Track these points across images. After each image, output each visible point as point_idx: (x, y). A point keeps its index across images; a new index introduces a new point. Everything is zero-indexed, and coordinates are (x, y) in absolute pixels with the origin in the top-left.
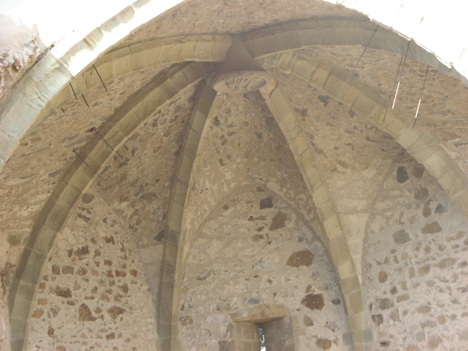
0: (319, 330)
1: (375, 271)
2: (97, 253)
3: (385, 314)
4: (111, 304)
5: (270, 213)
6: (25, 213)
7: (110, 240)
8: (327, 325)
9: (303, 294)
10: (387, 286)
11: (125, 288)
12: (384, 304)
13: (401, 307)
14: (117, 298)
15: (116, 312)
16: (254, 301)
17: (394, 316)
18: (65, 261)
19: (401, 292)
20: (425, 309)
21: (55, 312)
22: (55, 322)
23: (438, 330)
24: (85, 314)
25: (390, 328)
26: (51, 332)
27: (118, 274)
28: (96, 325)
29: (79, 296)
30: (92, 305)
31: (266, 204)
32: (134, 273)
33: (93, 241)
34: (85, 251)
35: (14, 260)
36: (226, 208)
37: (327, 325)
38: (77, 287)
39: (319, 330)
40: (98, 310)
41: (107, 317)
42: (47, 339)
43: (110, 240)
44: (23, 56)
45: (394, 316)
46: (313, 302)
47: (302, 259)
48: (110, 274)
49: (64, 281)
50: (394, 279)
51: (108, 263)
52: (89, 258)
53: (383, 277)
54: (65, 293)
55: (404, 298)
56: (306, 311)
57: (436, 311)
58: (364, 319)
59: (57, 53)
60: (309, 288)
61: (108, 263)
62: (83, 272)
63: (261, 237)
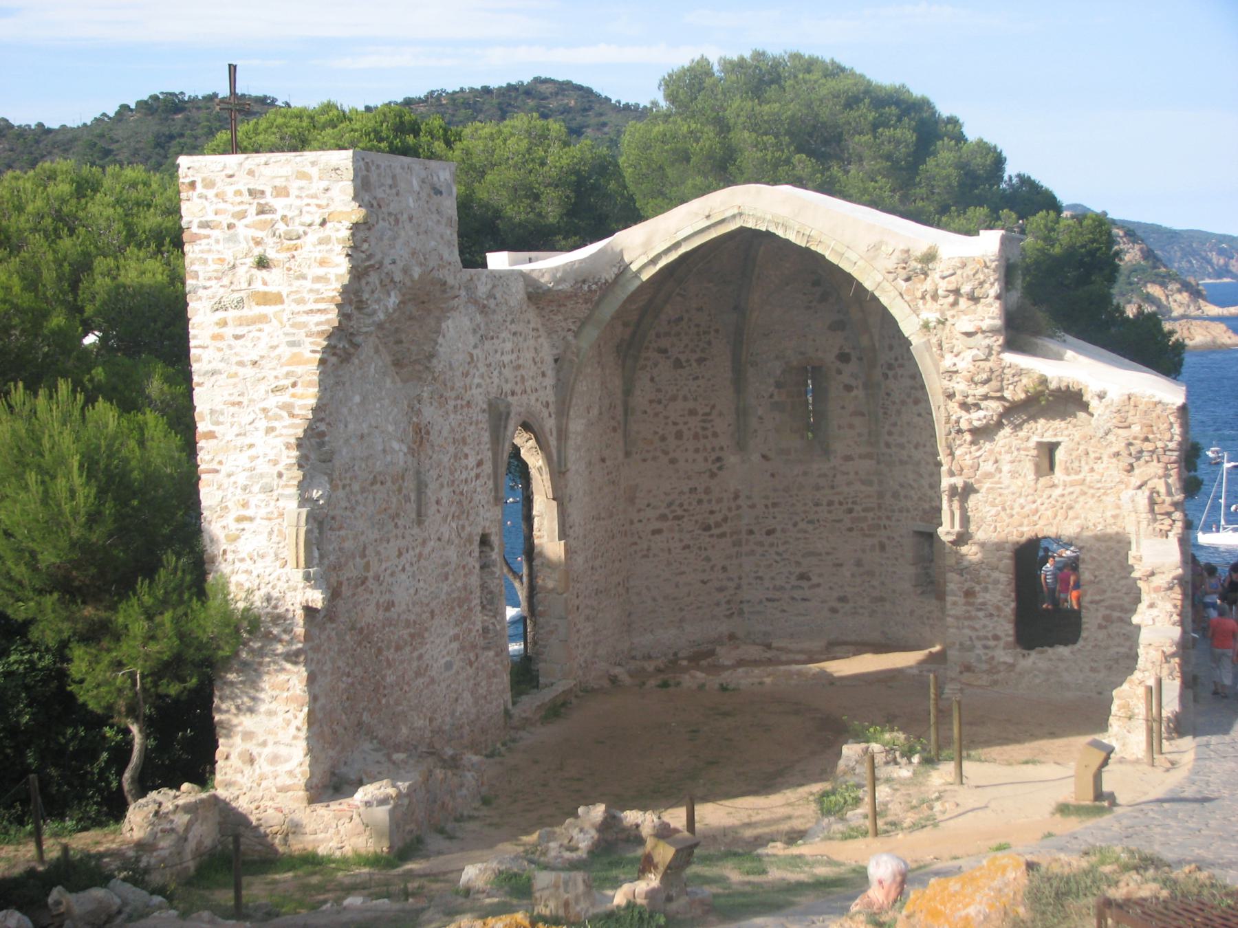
2: (690, 320)
3: (890, 373)
4: (696, 356)
6: (634, 307)
7: (700, 309)
8: (852, 375)
9: (836, 351)
11: (709, 343)
13: (900, 372)
14: (703, 350)
15: (700, 361)
16: (802, 353)
17: (895, 377)
19: (900, 361)
21: (656, 365)
24: (678, 364)
26: (652, 379)
27: (705, 333)
30: (683, 358)
32: (717, 331)
33: (687, 311)
34: (681, 319)
36: (787, 284)
37: (852, 375)
38: (673, 345)
40: (688, 361)
41: (694, 364)
43: (700, 309)
44: (609, 275)
45: (895, 377)
46: (844, 358)
48: (698, 334)
51: (697, 326)
54: (664, 351)
55: (901, 366)
56: (838, 364)
59: (634, 267)
60: (841, 347)
61: (697, 326)
63: (810, 308)
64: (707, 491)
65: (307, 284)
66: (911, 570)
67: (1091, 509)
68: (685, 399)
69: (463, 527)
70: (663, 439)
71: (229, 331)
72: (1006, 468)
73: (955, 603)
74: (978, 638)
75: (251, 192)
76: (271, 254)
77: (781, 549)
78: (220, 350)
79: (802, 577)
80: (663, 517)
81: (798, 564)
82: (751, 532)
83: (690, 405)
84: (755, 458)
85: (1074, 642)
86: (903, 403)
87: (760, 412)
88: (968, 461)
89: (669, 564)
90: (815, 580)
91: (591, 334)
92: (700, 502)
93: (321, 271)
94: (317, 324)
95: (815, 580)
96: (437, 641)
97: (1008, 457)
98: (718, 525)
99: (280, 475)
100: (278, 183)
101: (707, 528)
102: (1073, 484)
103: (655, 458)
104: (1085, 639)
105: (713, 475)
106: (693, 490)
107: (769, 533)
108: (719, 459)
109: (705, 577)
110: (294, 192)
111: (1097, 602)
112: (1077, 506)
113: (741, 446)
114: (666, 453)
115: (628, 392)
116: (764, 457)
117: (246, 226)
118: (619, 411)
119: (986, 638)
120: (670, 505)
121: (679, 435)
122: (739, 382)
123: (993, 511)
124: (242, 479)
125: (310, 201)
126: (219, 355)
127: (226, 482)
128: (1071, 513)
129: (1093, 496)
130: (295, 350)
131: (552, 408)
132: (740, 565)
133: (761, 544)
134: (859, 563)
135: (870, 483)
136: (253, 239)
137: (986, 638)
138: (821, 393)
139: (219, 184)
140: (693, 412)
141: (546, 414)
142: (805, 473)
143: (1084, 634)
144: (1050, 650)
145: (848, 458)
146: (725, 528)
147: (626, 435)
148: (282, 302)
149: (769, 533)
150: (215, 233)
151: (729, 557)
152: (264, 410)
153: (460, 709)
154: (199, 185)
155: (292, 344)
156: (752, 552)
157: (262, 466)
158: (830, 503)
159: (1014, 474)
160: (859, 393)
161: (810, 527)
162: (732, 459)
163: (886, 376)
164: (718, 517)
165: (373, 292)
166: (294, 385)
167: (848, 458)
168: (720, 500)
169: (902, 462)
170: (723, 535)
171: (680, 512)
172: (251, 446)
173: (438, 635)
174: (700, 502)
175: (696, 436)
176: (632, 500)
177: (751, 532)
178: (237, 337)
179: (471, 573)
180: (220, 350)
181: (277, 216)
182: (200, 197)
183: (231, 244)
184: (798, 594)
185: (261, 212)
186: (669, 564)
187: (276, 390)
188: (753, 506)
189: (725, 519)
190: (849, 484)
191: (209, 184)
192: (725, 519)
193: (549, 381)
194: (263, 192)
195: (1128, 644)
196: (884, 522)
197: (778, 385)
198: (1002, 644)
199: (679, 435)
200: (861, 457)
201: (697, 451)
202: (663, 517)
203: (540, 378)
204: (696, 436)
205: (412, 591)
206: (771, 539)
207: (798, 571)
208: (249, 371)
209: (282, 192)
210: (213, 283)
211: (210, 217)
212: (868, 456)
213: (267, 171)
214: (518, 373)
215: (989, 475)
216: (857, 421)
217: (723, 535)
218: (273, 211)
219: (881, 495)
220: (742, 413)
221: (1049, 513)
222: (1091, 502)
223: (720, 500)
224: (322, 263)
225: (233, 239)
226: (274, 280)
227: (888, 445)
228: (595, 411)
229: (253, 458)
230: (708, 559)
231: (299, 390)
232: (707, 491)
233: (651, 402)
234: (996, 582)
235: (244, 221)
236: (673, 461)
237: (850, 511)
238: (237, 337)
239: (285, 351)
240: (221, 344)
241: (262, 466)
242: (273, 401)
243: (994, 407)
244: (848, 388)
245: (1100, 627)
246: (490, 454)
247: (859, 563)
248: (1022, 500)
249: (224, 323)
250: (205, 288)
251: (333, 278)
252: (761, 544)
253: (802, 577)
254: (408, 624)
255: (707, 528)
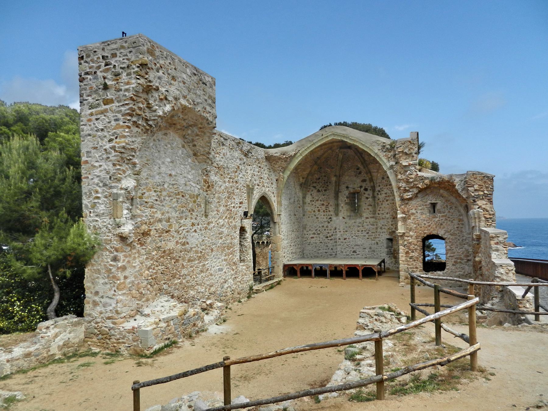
0: (366, 195)
1: (378, 185)
5: (358, 171)
7: (325, 176)
10: (380, 188)
12: (379, 191)
13: (382, 192)
15: (325, 190)
18: (315, 181)
20: (386, 194)
21: (312, 191)
22: (312, 193)
23: (388, 198)
25: (380, 196)
28: (321, 193)
29: (318, 187)
30: (320, 189)
31: (358, 169)
34: (319, 178)
35: (303, 182)
39: (366, 195)
42: (310, 196)
43: (325, 176)
45: (381, 194)
46: (366, 190)
47: (364, 181)
49: (315, 185)
50: (381, 187)
52: (321, 180)
53: (379, 186)
54: (315, 187)
57: (388, 194)
58: (376, 193)
62: (319, 183)
64: (327, 227)
65: (121, 93)
66: (386, 250)
67: (449, 225)
68: (321, 201)
69: (231, 222)
70: (314, 211)
71: (94, 118)
72: (419, 211)
73: (402, 256)
74: (411, 268)
75: (103, 57)
76: (109, 83)
77: (348, 244)
78: (90, 125)
79: (354, 252)
80: (314, 234)
81: (353, 248)
82: (340, 239)
83: (322, 202)
84: (341, 218)
85: (444, 270)
86: (383, 201)
87: (342, 205)
88: (406, 210)
89: (316, 247)
90: (358, 253)
91: (288, 173)
92: (325, 230)
93: (127, 87)
94: (125, 110)
95: (358, 253)
96: (215, 260)
97: (420, 208)
98: (330, 237)
99: (110, 178)
100: (112, 52)
101: (327, 237)
102: (442, 216)
103: (312, 217)
104: (448, 269)
105: (329, 223)
106: (323, 226)
107: (345, 239)
108: (330, 218)
109: (326, 251)
110: (118, 54)
111: (452, 257)
112: (444, 224)
113: (337, 215)
114: (315, 215)
115: (304, 198)
116: (344, 218)
117: (101, 72)
118: (301, 202)
119: (413, 268)
120: (316, 230)
121: (319, 211)
122: (337, 197)
123: (415, 226)
124: (96, 180)
125: (124, 58)
126: (89, 128)
127: (91, 182)
128: (442, 226)
129: (450, 220)
130: (117, 123)
131: (275, 195)
132: (337, 248)
133: (342, 242)
134: (370, 248)
135: (373, 225)
136: (103, 77)
137: (413, 268)
138: (359, 200)
139: (92, 56)
140: (323, 205)
141: (273, 196)
142: (355, 222)
143: (447, 267)
144: (435, 273)
145: (367, 218)
146: (332, 238)
147: (303, 209)
148: (113, 103)
149: (345, 239)
150: (89, 77)
151: (333, 246)
152: (105, 150)
153: (226, 286)
154: (85, 57)
155: (116, 120)
156: (340, 245)
157: (103, 174)
158: (362, 231)
159: (422, 214)
160: (370, 199)
161: (356, 238)
162: (334, 218)
163: (378, 194)
164: (330, 234)
165: (155, 101)
166: (116, 138)
167: (367, 218)
168: (331, 230)
169: (383, 218)
170: (332, 240)
171: (319, 232)
172: (100, 166)
173: (216, 258)
174: (325, 230)
175: (324, 211)
176: (305, 228)
177: (340, 239)
178: (97, 119)
179: (235, 238)
180: (90, 125)
181: (112, 66)
182: (86, 62)
183: (95, 81)
184: (352, 256)
185: (106, 65)
186: (316, 247)
187: (110, 141)
188: (340, 232)
189: (332, 235)
190: (367, 225)
191: (88, 56)
192: (332, 235)
193: (274, 186)
194: (107, 57)
195: (463, 271)
196: (378, 236)
197: (347, 198)
198: (418, 270)
199: (319, 211)
200: (371, 217)
201: (324, 215)
202: (314, 234)
203: (270, 184)
204: (324, 211)
205: (200, 240)
206: (345, 241)
207: (353, 250)
208: (99, 133)
209: (114, 55)
210: (89, 98)
211: (88, 70)
212: (373, 217)
213: (109, 48)
214: (262, 180)
215: (413, 214)
216: (370, 208)
217: (332, 240)
218: (110, 64)
219: (377, 228)
220: (337, 205)
221: (434, 226)
222: (449, 223)
223: (331, 230)
224: (128, 83)
225: (96, 78)
226: (110, 95)
227: (379, 214)
228: (292, 200)
229: (101, 171)
230: (327, 246)
231: (118, 140)
232: (327, 227)
233: (311, 201)
234: (416, 249)
235: (100, 70)
236: (317, 218)
237: (368, 233)
238: (97, 119)
239: (113, 123)
240: (91, 123)
241: (103, 174)
242: (108, 146)
243: (415, 191)
244: (367, 198)
245: (453, 265)
246: (246, 201)
247: (370, 248)
248: (425, 222)
249: (91, 114)
250: (86, 100)
251: (131, 89)
252: (342, 242)
253: (354, 252)
254: (197, 252)
255: (327, 237)
